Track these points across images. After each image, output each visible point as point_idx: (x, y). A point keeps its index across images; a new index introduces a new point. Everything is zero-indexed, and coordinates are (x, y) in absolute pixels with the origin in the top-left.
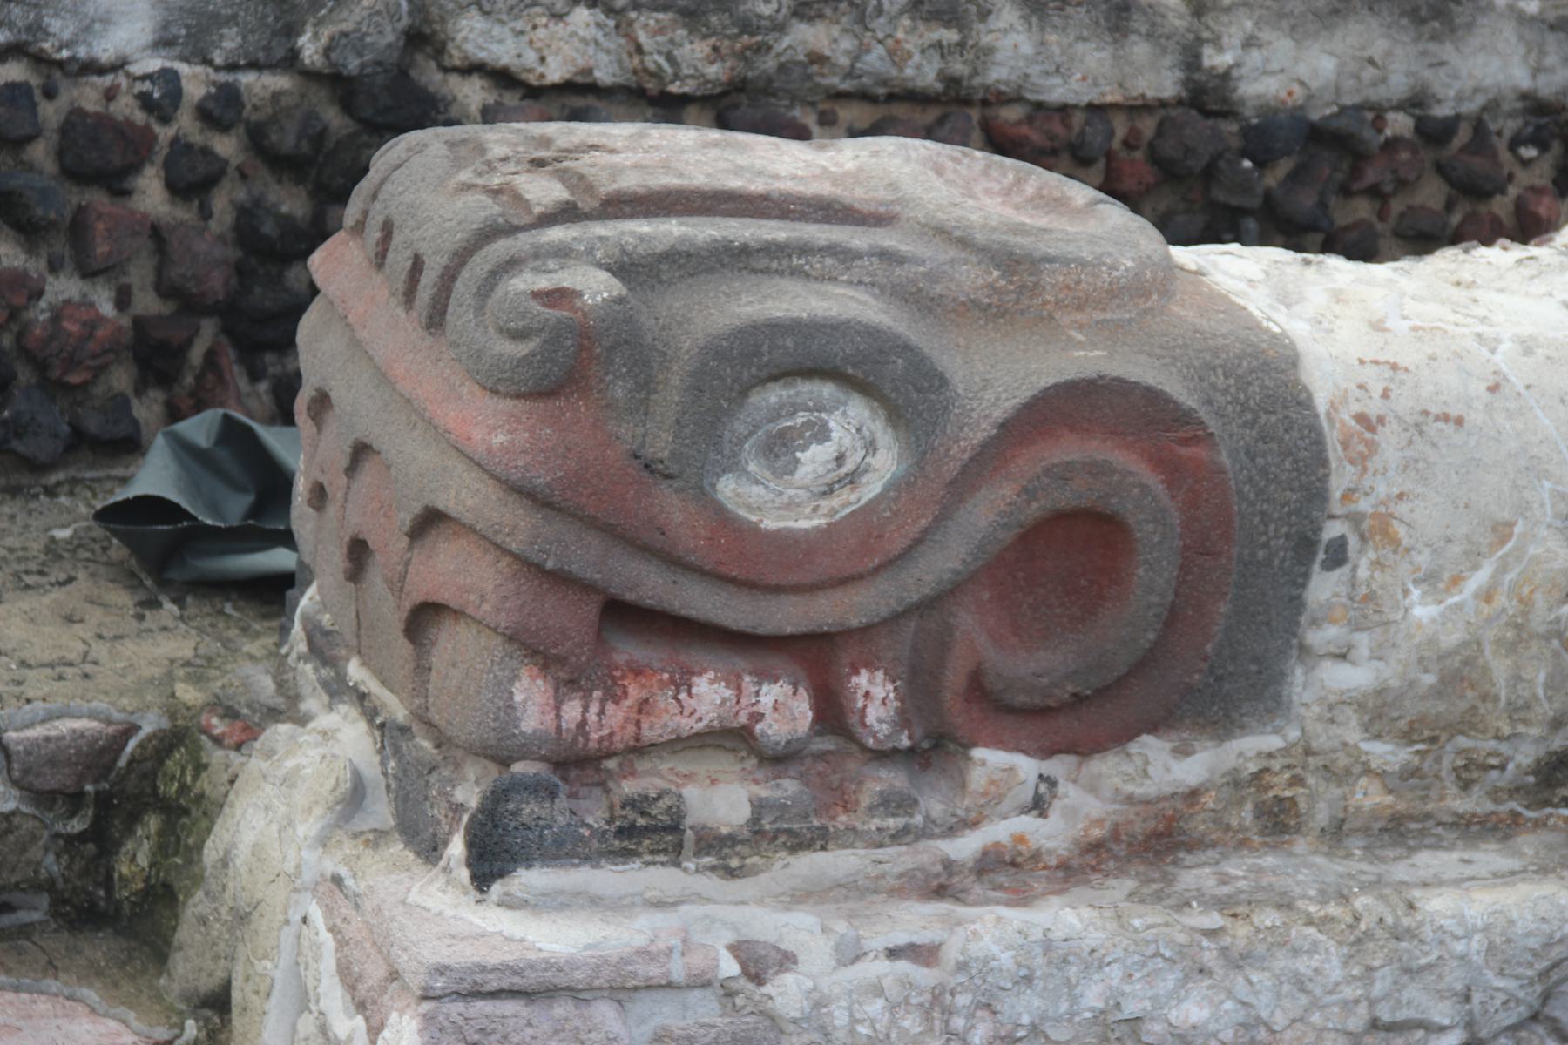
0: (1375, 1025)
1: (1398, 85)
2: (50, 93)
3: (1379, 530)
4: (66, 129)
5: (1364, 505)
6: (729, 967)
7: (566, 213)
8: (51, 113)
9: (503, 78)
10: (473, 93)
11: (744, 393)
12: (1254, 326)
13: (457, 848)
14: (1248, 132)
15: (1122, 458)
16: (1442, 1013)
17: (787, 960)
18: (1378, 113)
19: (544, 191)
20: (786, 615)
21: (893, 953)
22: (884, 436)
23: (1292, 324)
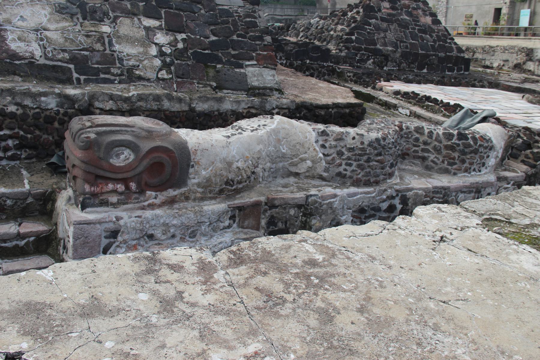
0: (198, 222)
1: (216, 108)
2: (43, 113)
3: (198, 163)
4: (45, 117)
5: (196, 160)
6: (114, 219)
7: (91, 127)
8: (43, 115)
9: (101, 109)
10: (98, 111)
11: (113, 148)
12: (182, 139)
13: (80, 206)
14: (197, 114)
15: (162, 155)
16: (206, 220)
17: (122, 218)
18: (214, 112)
19: (88, 124)
20: (120, 176)
21: (136, 217)
22: (131, 153)
23: (188, 139)
